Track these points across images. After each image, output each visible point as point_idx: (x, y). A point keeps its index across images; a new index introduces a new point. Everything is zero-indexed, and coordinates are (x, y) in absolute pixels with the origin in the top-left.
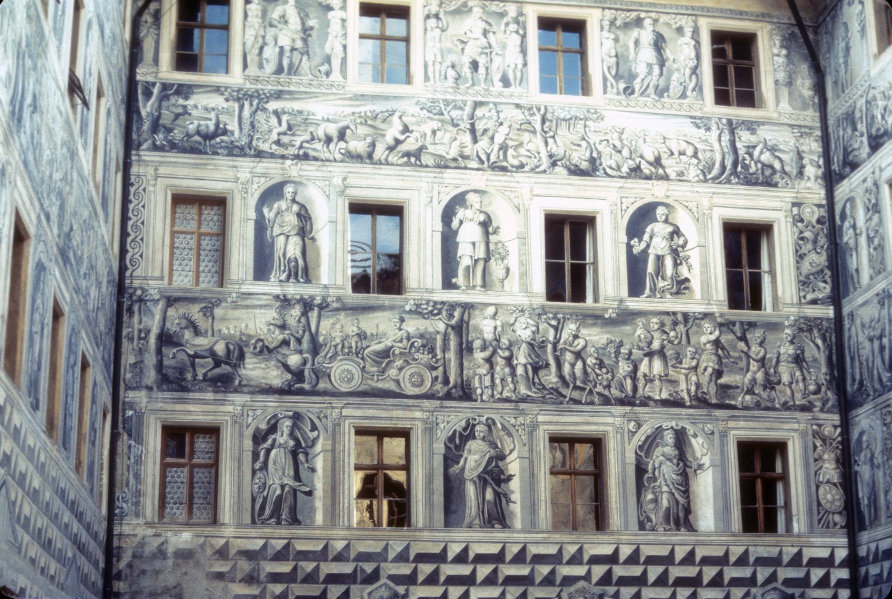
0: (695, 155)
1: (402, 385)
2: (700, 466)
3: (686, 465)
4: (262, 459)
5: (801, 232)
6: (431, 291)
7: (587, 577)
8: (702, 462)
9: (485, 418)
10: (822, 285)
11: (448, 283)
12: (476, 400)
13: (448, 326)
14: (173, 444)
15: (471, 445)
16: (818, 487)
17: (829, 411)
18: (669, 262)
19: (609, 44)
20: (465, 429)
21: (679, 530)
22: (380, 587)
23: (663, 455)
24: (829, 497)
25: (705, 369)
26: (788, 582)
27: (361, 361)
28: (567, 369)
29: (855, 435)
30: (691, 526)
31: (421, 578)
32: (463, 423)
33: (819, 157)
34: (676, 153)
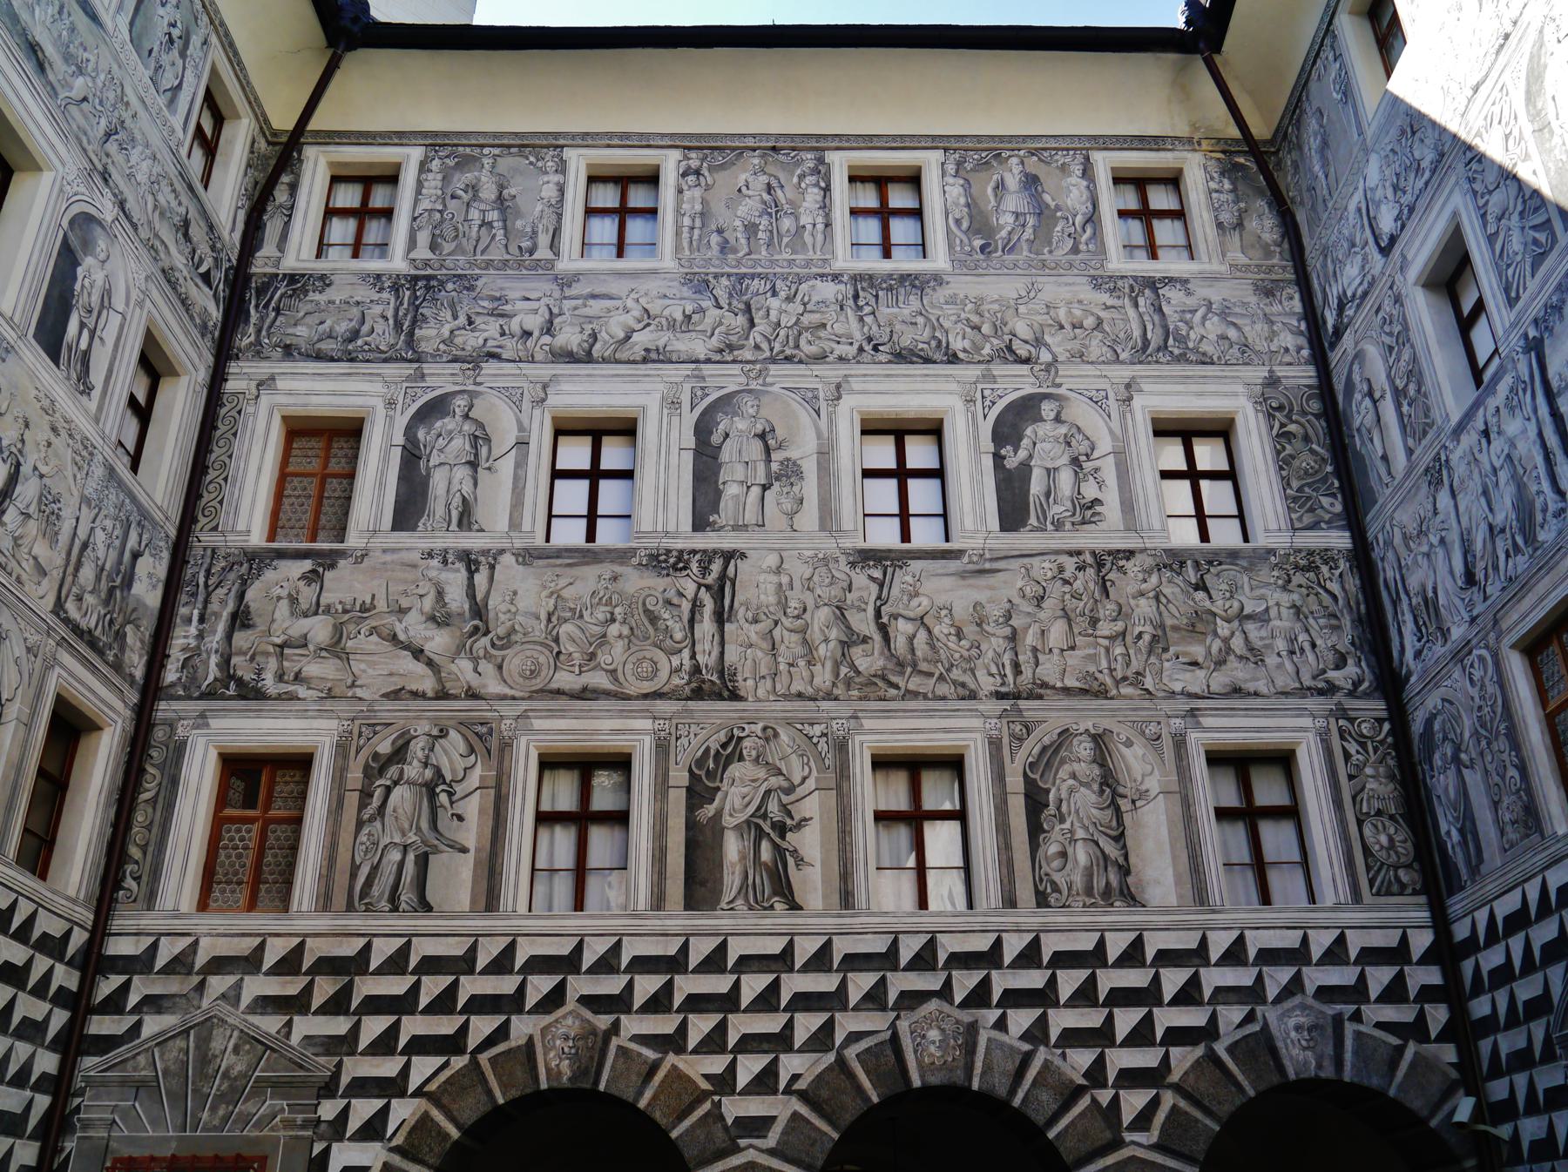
0: (1100, 322)
1: (621, 679)
2: (1143, 794)
3: (1115, 794)
4: (376, 801)
5: (1282, 425)
6: (676, 535)
7: (946, 992)
8: (1143, 788)
9: (761, 725)
10: (1325, 501)
11: (700, 523)
12: (746, 700)
13: (700, 586)
14: (238, 784)
15: (735, 770)
16: (1360, 823)
17: (1366, 695)
18: (1065, 479)
19: (956, 191)
20: (724, 746)
21: (1112, 905)
22: (564, 1017)
23: (1074, 776)
24: (1384, 839)
25: (1140, 636)
26: (1325, 993)
27: (553, 644)
28: (900, 644)
29: (1417, 727)
30: (1133, 899)
31: (638, 1001)
32: (722, 737)
33: (1299, 321)
34: (1068, 327)
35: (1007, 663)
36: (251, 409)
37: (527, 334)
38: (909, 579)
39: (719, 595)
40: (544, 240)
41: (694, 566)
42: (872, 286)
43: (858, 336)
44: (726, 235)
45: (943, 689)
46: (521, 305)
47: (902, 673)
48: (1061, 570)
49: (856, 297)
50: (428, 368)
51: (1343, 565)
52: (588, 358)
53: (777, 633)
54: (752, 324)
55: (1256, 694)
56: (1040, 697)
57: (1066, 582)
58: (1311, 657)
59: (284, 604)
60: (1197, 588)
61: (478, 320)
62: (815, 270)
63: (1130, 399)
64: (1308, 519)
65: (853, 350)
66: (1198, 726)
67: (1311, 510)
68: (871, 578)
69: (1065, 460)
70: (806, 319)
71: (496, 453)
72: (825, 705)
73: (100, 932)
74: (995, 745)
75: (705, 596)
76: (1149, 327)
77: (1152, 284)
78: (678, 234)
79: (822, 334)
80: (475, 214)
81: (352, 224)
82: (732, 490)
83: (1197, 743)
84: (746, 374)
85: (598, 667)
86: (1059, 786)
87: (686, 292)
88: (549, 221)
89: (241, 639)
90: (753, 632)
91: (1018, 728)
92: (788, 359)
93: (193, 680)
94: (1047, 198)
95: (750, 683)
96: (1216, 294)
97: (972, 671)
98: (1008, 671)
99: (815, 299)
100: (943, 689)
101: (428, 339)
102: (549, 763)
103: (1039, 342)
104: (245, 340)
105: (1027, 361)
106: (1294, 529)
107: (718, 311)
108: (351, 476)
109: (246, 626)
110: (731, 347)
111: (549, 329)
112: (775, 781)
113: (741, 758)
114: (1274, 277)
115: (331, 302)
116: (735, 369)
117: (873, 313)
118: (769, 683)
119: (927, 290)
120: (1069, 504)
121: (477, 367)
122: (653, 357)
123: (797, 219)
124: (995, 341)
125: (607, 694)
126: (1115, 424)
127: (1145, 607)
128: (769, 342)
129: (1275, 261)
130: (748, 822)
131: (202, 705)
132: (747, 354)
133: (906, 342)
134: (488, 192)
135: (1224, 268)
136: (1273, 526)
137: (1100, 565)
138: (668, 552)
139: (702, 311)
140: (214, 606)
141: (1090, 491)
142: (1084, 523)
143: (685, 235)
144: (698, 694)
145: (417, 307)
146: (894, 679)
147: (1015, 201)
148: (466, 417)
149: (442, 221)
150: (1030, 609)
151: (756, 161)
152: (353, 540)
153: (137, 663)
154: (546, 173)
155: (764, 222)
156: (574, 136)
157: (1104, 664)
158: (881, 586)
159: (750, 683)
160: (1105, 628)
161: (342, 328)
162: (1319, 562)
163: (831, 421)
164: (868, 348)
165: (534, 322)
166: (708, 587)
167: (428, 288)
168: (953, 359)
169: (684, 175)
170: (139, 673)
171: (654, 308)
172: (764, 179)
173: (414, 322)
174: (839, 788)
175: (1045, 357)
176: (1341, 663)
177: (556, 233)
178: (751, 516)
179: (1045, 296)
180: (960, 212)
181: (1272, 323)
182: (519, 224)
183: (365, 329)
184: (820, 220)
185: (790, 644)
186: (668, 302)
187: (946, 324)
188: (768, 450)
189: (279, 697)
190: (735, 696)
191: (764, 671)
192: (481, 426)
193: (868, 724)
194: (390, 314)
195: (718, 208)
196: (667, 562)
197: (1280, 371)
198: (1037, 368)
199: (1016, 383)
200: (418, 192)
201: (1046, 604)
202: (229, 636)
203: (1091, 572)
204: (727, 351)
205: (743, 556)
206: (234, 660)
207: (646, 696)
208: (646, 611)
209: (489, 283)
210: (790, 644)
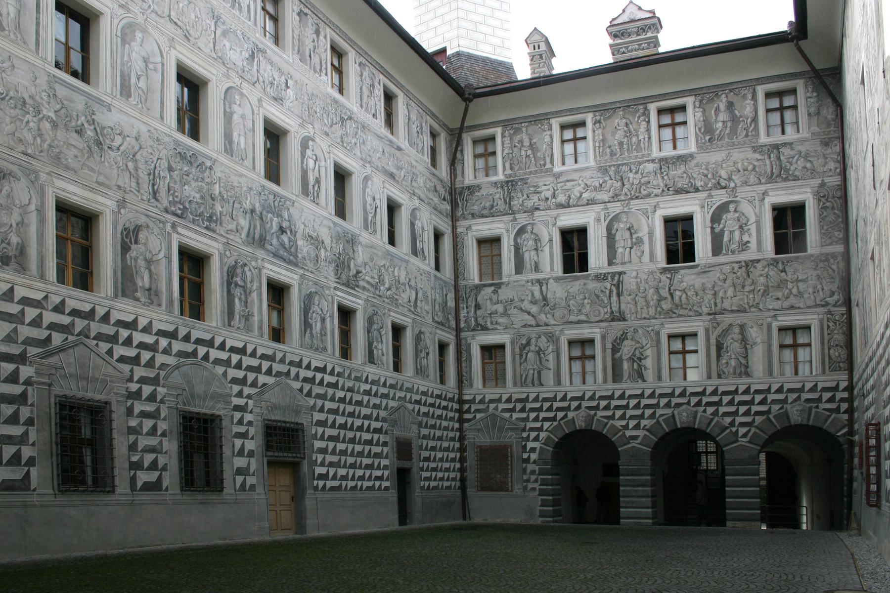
6: (603, 268)
10: (836, 233)
11: (610, 263)
15: (626, 342)
18: (737, 235)
19: (699, 114)
20: (622, 335)
28: (677, 299)
32: (621, 333)
34: (742, 171)
35: (712, 303)
37: (547, 199)
38: (680, 277)
39: (618, 288)
40: (548, 160)
41: (609, 278)
42: (667, 163)
43: (662, 185)
44: (612, 148)
45: (691, 313)
46: (544, 188)
47: (677, 309)
48: (733, 269)
49: (661, 168)
50: (517, 216)
51: (840, 258)
52: (569, 206)
53: (637, 299)
54: (623, 185)
55: (799, 308)
56: (723, 314)
57: (735, 273)
58: (821, 293)
60: (782, 271)
61: (531, 196)
62: (645, 159)
63: (764, 199)
64: (828, 241)
65: (660, 191)
66: (777, 320)
67: (830, 238)
68: (667, 277)
69: (737, 227)
70: (643, 180)
71: (543, 245)
72: (653, 321)
74: (707, 331)
75: (614, 288)
76: (774, 167)
77: (777, 147)
78: (595, 150)
79: (649, 186)
80: (523, 153)
82: (620, 250)
83: (775, 325)
84: (623, 205)
85: (582, 314)
86: (728, 341)
87: (600, 175)
88: (548, 152)
90: (629, 299)
91: (715, 324)
92: (637, 198)
94: (736, 112)
95: (629, 315)
96: (803, 149)
97: (701, 306)
98: (713, 306)
99: (646, 171)
100: (691, 313)
101: (515, 205)
102: (571, 343)
103: (730, 179)
105: (725, 188)
106: (822, 246)
107: (611, 181)
110: (617, 195)
111: (554, 196)
112: (638, 345)
113: (627, 339)
114: (830, 136)
116: (619, 204)
117: (667, 175)
118: (635, 315)
119: (688, 162)
120: (737, 244)
121: (533, 214)
122: (591, 202)
123: (638, 137)
124: (713, 181)
125: (586, 322)
126: (757, 211)
127: (762, 280)
128: (630, 191)
129: (832, 128)
130: (630, 358)
132: (623, 198)
133: (680, 185)
134: (526, 143)
135: (807, 135)
136: (814, 245)
137: (747, 266)
138: (601, 274)
139: (605, 182)
141: (746, 238)
142: (743, 250)
143: (597, 150)
144: (613, 320)
145: (510, 193)
146: (675, 311)
147: (723, 116)
148: (532, 232)
149: (513, 157)
150: (721, 284)
151: (621, 113)
154: (545, 131)
155: (625, 140)
157: (746, 301)
158: (671, 280)
159: (629, 315)
160: (747, 289)
161: (488, 204)
162: (830, 257)
163: (653, 221)
164: (665, 189)
165: (549, 194)
166: (614, 285)
167: (512, 185)
168: (697, 190)
169: (595, 124)
171: (589, 183)
172: (624, 121)
173: (510, 199)
174: (657, 346)
175: (732, 185)
176: (832, 294)
178: (626, 259)
179: (733, 159)
180: (702, 124)
181: (826, 158)
182: (539, 154)
183: (495, 204)
184: (646, 136)
185: (641, 302)
186: (593, 180)
187: (695, 176)
188: (631, 234)
190: (624, 320)
191: (633, 311)
192: (537, 235)
193: (666, 326)
194: (502, 197)
195: (609, 137)
196: (601, 277)
197: (827, 180)
198: (729, 190)
199: (721, 196)
201: (728, 281)
203: (744, 269)
204: (615, 197)
205: (625, 273)
207: (597, 322)
208: (595, 294)
209: (532, 180)
210: (641, 302)
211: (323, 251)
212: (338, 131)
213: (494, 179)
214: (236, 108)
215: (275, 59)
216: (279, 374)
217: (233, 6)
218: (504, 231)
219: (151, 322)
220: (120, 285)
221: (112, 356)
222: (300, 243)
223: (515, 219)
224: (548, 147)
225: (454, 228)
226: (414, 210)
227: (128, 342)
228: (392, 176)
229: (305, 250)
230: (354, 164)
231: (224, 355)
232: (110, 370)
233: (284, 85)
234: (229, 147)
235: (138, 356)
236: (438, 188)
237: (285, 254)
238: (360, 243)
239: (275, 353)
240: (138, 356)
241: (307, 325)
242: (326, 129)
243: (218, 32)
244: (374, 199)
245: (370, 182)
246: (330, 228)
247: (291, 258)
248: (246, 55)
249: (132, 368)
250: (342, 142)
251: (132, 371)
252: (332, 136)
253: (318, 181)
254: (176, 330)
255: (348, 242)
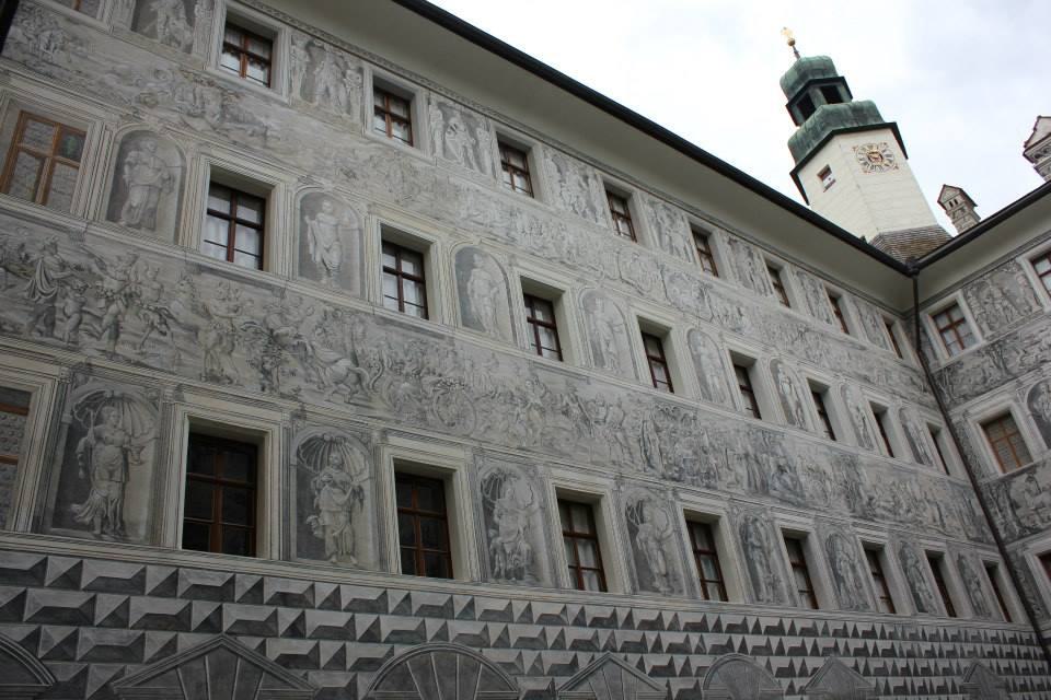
36: (966, 427)
40: (1033, 303)
59: (1026, 493)
61: (1028, 350)
73: (1038, 632)
81: (951, 332)
89: (1019, 512)
93: (1012, 535)
104: (948, 401)
108: (1018, 432)
109: (1018, 507)
115: (968, 371)
131: (1020, 542)
134: (997, 294)
140: (1002, 505)
152: (1037, 459)
153: (990, 536)
156: (1015, 251)
161: (979, 379)
167: (1000, 346)
170: (993, 540)
177: (1036, 297)
182: (1018, 301)
183: (987, 374)
189: (1047, 529)
200: (971, 309)
202: (1014, 513)
206: (1023, 521)
209: (1023, 332)
211: (828, 483)
212: (800, 346)
213: (974, 347)
214: (701, 349)
215: (722, 290)
216: (827, 651)
217: (672, 253)
218: (1011, 402)
219: (676, 615)
220: (635, 576)
221: (644, 671)
222: (803, 479)
223: (1020, 383)
224: (1027, 289)
225: (948, 421)
226: (901, 410)
227: (657, 647)
228: (866, 379)
229: (810, 486)
230: (827, 377)
231: (761, 641)
232: (646, 690)
233: (737, 315)
234: (706, 392)
235: (671, 664)
236: (915, 379)
237: (792, 496)
238: (861, 464)
239: (815, 625)
240: (671, 664)
241: (838, 578)
242: (789, 347)
243: (666, 279)
244: (858, 409)
245: (848, 392)
246: (826, 454)
247: (799, 499)
248: (696, 294)
249: (668, 681)
250: (808, 357)
251: (668, 685)
252: (797, 353)
253: (799, 405)
254: (704, 619)
255: (849, 465)
